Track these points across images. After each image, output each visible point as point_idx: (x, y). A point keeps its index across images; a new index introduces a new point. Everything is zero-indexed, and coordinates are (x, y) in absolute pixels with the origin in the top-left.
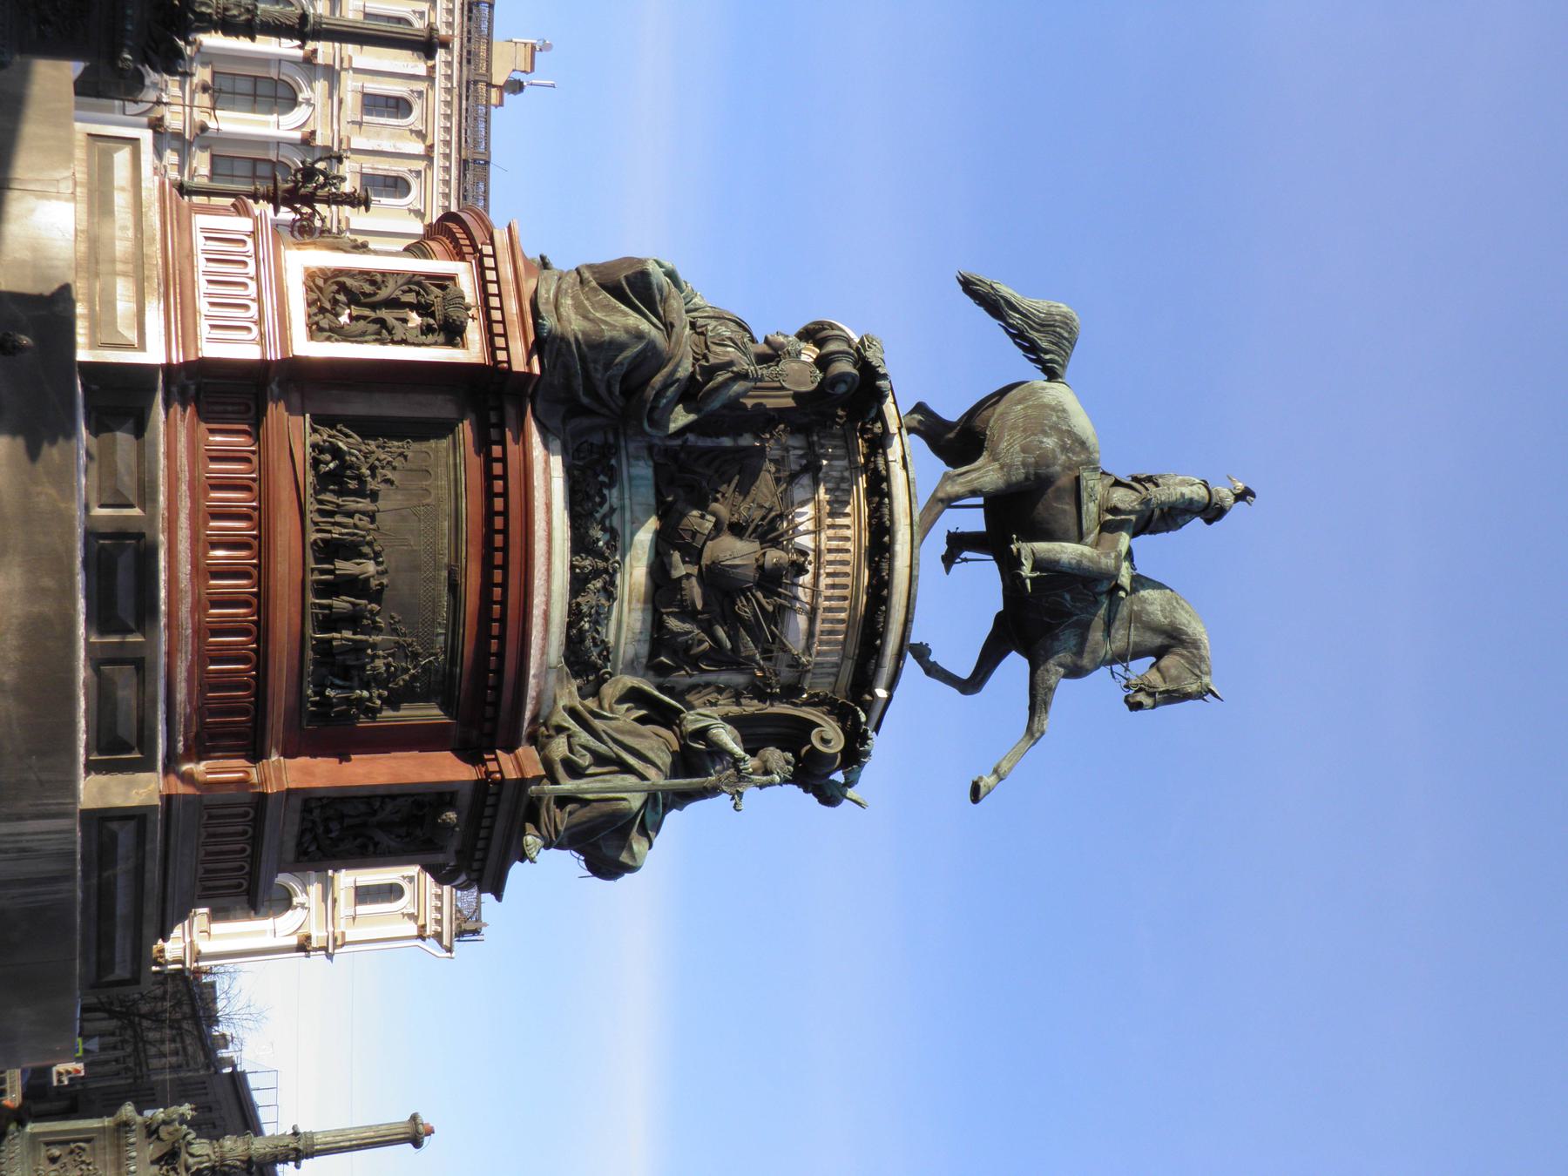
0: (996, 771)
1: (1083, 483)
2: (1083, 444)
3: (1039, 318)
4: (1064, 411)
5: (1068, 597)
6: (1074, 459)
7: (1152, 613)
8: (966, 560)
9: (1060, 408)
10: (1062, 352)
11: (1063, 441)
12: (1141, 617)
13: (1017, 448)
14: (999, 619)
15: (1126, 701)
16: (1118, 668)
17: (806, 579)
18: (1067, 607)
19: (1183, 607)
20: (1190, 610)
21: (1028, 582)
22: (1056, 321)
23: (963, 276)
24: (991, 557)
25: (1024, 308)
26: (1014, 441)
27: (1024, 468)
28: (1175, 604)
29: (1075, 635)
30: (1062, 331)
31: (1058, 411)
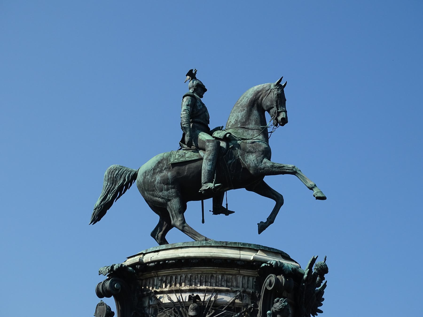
0: (311, 189)
1: (176, 161)
2: (159, 163)
3: (109, 186)
4: (145, 172)
5: (230, 162)
6: (165, 166)
7: (242, 116)
8: (227, 204)
9: (144, 174)
10: (125, 173)
11: (158, 172)
12: (243, 122)
13: (161, 194)
14: (248, 189)
15: (283, 125)
16: (269, 130)
17: (201, 296)
18: (235, 161)
19: (241, 101)
20: (242, 97)
21: (216, 185)
22: (111, 177)
23: (91, 222)
24: (225, 192)
25: (105, 193)
26: (158, 195)
27: (169, 190)
28: (239, 105)
29: (248, 156)
30: (115, 174)
31: (146, 175)
